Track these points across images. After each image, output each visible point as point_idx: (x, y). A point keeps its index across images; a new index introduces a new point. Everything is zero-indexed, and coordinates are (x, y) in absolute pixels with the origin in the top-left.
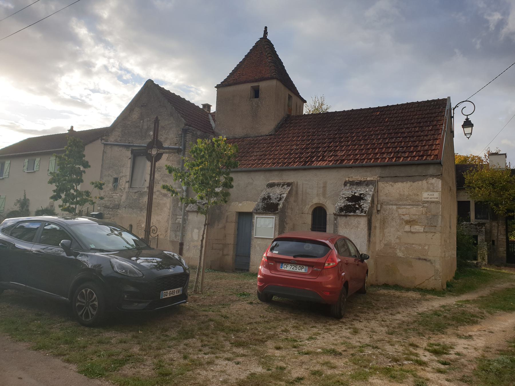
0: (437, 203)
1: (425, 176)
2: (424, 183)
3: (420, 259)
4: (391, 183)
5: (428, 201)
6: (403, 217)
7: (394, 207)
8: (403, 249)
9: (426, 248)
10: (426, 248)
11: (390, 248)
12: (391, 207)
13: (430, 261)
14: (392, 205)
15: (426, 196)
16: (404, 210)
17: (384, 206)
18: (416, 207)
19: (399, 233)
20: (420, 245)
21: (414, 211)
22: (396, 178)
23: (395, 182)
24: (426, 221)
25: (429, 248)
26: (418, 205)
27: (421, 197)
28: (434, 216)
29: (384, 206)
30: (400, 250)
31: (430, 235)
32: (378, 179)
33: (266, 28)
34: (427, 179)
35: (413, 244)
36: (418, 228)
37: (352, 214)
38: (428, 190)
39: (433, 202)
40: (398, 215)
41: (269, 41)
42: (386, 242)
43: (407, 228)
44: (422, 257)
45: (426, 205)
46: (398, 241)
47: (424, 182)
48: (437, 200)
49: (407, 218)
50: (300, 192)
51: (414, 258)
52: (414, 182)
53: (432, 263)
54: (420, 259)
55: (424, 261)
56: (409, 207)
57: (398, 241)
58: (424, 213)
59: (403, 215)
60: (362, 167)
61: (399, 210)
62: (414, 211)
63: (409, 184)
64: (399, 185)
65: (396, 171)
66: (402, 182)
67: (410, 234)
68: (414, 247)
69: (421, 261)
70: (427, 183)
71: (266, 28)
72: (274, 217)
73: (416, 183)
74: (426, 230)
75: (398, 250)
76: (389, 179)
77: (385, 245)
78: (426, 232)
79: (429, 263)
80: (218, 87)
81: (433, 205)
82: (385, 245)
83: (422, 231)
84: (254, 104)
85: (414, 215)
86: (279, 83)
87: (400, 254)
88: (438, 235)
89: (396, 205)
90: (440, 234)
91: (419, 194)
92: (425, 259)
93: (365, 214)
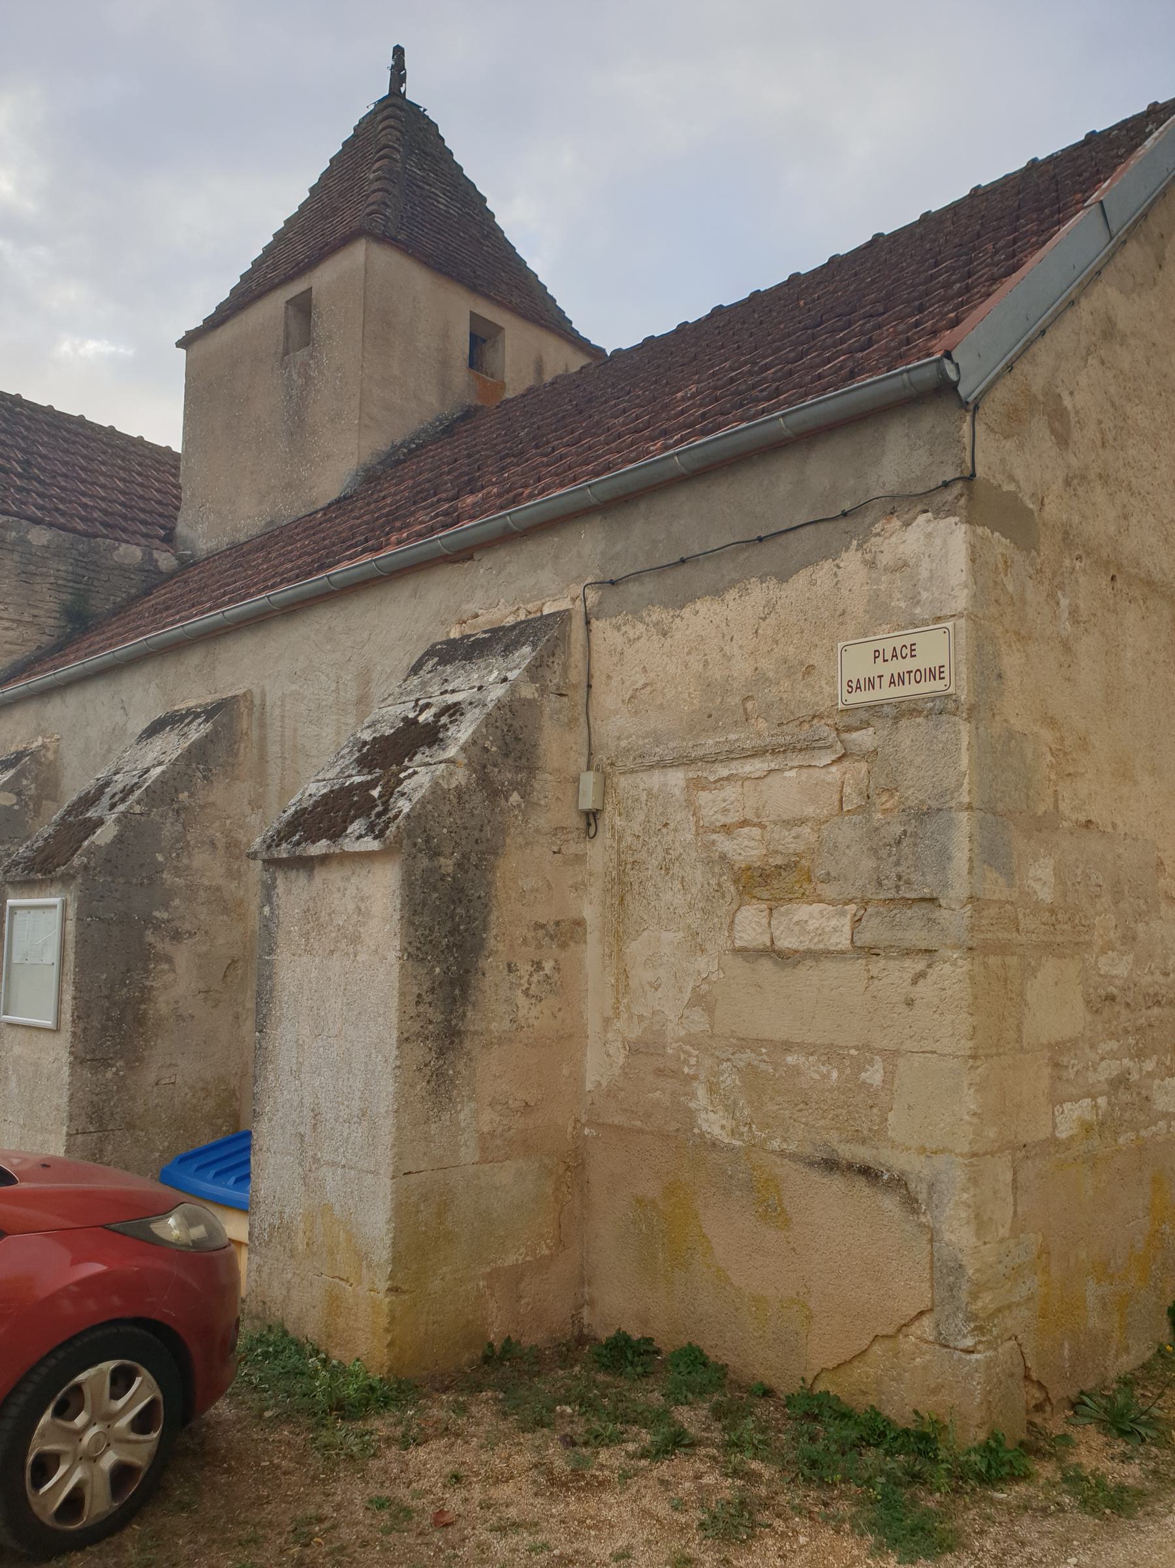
0: (939, 709)
1: (850, 519)
2: (847, 574)
3: (831, 1165)
4: (657, 614)
5: (874, 709)
6: (725, 844)
7: (676, 779)
8: (729, 1080)
9: (874, 1075)
10: (874, 1075)
11: (659, 1072)
12: (655, 780)
13: (898, 1183)
14: (662, 765)
15: (857, 667)
16: (730, 792)
17: (624, 782)
18: (797, 760)
19: (702, 964)
20: (831, 1053)
21: (792, 795)
22: (680, 575)
23: (679, 601)
24: (868, 863)
25: (890, 1076)
26: (808, 747)
27: (831, 682)
28: (923, 814)
29: (624, 782)
30: (712, 1089)
31: (895, 974)
32: (593, 597)
33: (399, 52)
34: (867, 535)
35: (788, 1047)
36: (817, 922)
37: (320, 847)
38: (879, 613)
39: (906, 710)
40: (701, 830)
41: (415, 114)
42: (634, 1033)
43: (751, 925)
44: (848, 1152)
45: (864, 738)
46: (698, 1021)
47: (851, 560)
48: (937, 685)
49: (745, 849)
50: (274, 749)
51: (793, 1157)
52: (783, 577)
53: (911, 1203)
54: (831, 1165)
55: (861, 1182)
56: (756, 767)
57: (698, 1021)
58: (853, 801)
59: (726, 829)
60: (508, 537)
61: (704, 797)
62: (792, 795)
63: (759, 592)
64: (702, 618)
65: (689, 521)
66: (717, 592)
67: (766, 966)
68: (796, 1071)
69: (837, 1183)
70: (871, 564)
71: (399, 52)
72: (56, 901)
73: (800, 580)
74: (866, 938)
75: (701, 1092)
76: (649, 586)
77: (634, 1050)
78: (870, 952)
79: (890, 1203)
80: (186, 342)
81: (910, 734)
82: (634, 1050)
83: (842, 941)
84: (295, 377)
85: (788, 824)
86: (386, 259)
87: (713, 1123)
88: (952, 974)
89: (683, 761)
90: (965, 966)
91: (816, 659)
92: (866, 1172)
93: (371, 844)
